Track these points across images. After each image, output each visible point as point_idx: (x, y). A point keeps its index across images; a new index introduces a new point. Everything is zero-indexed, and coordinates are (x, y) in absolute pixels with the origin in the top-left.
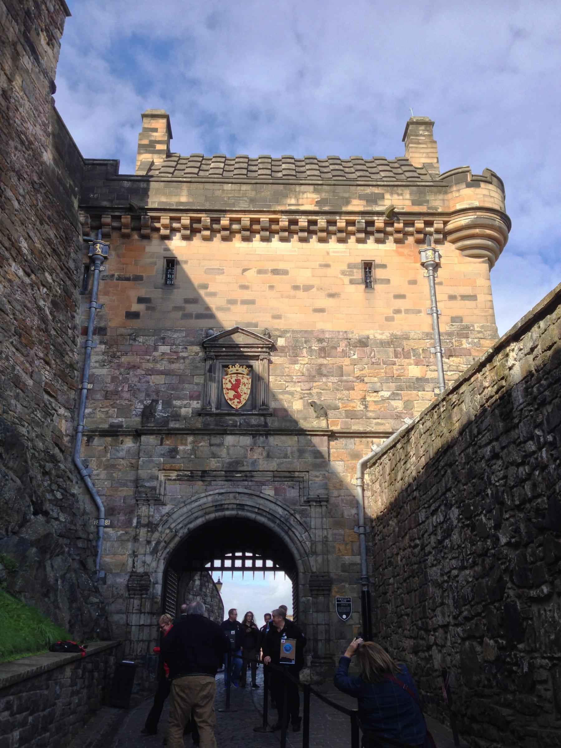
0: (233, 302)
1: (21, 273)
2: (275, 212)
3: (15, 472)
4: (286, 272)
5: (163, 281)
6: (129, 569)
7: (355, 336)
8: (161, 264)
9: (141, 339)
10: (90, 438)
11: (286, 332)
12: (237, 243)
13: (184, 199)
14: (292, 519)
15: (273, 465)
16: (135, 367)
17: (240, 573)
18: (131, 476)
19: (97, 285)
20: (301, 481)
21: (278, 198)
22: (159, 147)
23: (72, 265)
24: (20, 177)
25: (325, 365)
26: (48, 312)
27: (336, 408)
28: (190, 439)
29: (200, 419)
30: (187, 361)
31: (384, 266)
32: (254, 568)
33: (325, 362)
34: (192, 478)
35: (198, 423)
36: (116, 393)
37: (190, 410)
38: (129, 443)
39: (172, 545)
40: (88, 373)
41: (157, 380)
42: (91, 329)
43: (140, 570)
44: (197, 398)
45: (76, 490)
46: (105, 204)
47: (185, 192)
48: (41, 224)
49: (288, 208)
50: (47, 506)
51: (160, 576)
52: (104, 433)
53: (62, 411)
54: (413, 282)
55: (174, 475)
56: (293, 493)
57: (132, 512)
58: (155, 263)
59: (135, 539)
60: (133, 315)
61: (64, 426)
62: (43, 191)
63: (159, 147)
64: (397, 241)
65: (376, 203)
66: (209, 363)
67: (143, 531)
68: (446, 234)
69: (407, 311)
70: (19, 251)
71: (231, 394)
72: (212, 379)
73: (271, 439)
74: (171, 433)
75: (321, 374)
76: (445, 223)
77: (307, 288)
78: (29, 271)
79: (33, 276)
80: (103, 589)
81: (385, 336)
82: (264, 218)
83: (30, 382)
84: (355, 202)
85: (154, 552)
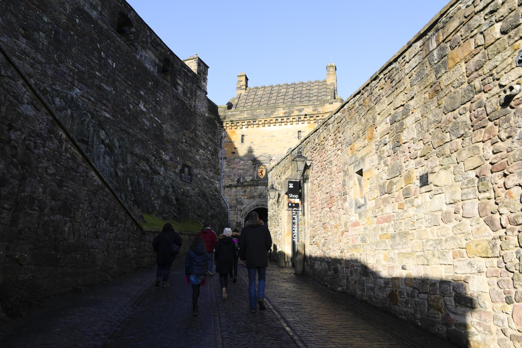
1: (203, 151)
4: (275, 136)
10: (225, 188)
13: (245, 116)
16: (235, 168)
24: (200, 126)
28: (249, 187)
34: (250, 198)
36: (230, 176)
38: (234, 189)
41: (241, 171)
49: (275, 116)
52: (228, 187)
53: (217, 182)
57: (236, 207)
59: (237, 214)
65: (301, 111)
70: (201, 145)
72: (255, 170)
74: (244, 186)
85: (242, 217)
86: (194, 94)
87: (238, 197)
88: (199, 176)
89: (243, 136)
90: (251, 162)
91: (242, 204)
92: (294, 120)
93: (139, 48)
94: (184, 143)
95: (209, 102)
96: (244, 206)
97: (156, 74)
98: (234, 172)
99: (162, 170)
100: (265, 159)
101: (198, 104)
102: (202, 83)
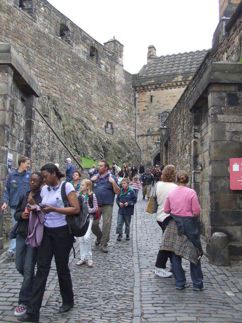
0: (164, 105)
8: (150, 97)
12: (165, 91)
13: (153, 81)
22: (152, 57)
38: (146, 138)
52: (141, 136)
60: (145, 110)
63: (152, 57)
74: (153, 135)
82: (170, 84)
86: (113, 68)
88: (119, 129)
89: (152, 97)
91: (152, 149)
93: (74, 44)
95: (125, 72)
97: (86, 60)
99: (92, 127)
101: (117, 75)
102: (119, 59)
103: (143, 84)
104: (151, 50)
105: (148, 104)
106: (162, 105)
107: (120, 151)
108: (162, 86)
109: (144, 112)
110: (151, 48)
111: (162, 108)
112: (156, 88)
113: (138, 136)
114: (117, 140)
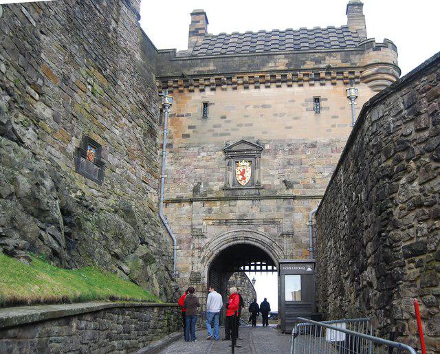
0: (240, 125)
1: (127, 122)
2: (262, 72)
3: (130, 224)
4: (269, 106)
5: (202, 116)
6: (190, 270)
7: (309, 142)
9: (191, 149)
11: (270, 141)
14: (274, 244)
15: (263, 216)
17: (265, 273)
18: (189, 223)
19: (167, 120)
20: (278, 224)
21: (264, 63)
23: (153, 111)
25: (292, 159)
26: (141, 139)
27: (298, 183)
28: (218, 203)
29: (223, 192)
30: (216, 160)
31: (326, 99)
32: (267, 270)
33: (290, 157)
35: (223, 195)
36: (179, 179)
37: (218, 187)
38: (187, 206)
39: (211, 258)
40: (164, 169)
42: (165, 145)
43: (196, 271)
44: (222, 180)
45: (162, 231)
46: (169, 74)
47: (212, 64)
48: (136, 93)
50: (147, 240)
51: (206, 274)
53: (152, 190)
54: (343, 108)
55: (211, 222)
56: (274, 231)
57: (190, 242)
58: (196, 106)
59: (193, 256)
61: (154, 199)
62: (136, 75)
63: (200, 32)
64: (334, 84)
66: (228, 161)
67: (196, 251)
68: (363, 78)
69: (339, 126)
71: (241, 177)
73: (262, 202)
74: (208, 200)
75: (289, 164)
76: (361, 72)
77: (282, 115)
78: (131, 120)
79: (133, 123)
80: (178, 279)
81: (326, 141)
82: (257, 76)
83: (135, 178)
84: (308, 62)
85: (203, 262)
87: (194, 222)
88: (118, 171)
89: (206, 105)
90: (221, 153)
91: (203, 236)
92: (306, 78)
94: (90, 94)
96: (207, 240)
98: (188, 172)
99: (29, 135)
100: (250, 147)
103: (187, 72)
104: (198, 18)
105: (198, 123)
106: (233, 125)
107: (119, 237)
108: (234, 79)
109: (183, 140)
110: (199, 17)
111: (233, 133)
112: (220, 84)
113: (167, 202)
114: (112, 200)
